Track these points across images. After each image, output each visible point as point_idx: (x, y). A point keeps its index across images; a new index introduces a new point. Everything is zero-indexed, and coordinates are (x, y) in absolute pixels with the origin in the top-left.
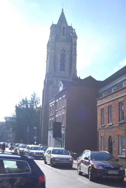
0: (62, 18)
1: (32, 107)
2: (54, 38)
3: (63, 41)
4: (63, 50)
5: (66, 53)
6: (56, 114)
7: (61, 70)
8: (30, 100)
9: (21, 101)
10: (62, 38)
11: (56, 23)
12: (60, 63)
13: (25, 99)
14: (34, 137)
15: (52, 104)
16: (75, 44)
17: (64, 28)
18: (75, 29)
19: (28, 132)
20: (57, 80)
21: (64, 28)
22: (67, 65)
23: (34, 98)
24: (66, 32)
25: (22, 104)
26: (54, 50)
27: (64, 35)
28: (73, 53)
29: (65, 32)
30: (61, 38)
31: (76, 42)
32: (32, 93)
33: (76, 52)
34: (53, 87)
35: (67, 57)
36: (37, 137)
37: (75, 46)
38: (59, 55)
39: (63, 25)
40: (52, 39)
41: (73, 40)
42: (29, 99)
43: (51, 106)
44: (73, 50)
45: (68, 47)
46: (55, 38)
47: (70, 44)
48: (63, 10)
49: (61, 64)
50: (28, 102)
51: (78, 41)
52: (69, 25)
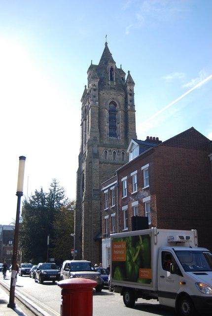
0: (107, 56)
1: (51, 203)
2: (96, 83)
3: (109, 93)
4: (112, 102)
7: (111, 134)
8: (49, 192)
9: (34, 194)
11: (97, 62)
13: (39, 191)
14: (72, 252)
15: (109, 188)
16: (132, 94)
17: (112, 69)
19: (48, 244)
20: (106, 151)
21: (112, 69)
22: (120, 126)
23: (55, 190)
24: (116, 76)
25: (35, 199)
27: (112, 79)
28: (129, 107)
29: (114, 76)
32: (52, 182)
33: (133, 106)
34: (100, 163)
35: (120, 113)
36: (76, 251)
38: (106, 110)
41: (128, 88)
42: (47, 191)
44: (129, 102)
45: (120, 99)
48: (106, 43)
51: (136, 89)
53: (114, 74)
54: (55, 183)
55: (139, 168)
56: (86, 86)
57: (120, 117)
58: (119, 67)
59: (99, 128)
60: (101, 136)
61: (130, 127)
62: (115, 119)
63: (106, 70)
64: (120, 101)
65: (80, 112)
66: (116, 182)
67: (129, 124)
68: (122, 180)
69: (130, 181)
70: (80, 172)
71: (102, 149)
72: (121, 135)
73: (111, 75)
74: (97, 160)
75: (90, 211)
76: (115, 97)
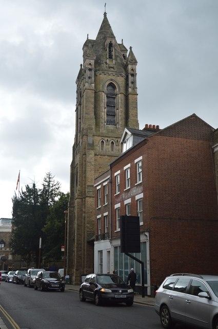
0: (105, 27)
1: (45, 202)
4: (111, 85)
6: (113, 204)
8: (42, 188)
9: (25, 190)
11: (93, 37)
13: (31, 187)
16: (134, 75)
17: (111, 45)
20: (103, 142)
21: (111, 45)
22: (120, 112)
23: (49, 185)
24: (115, 53)
27: (111, 57)
28: (130, 90)
29: (113, 53)
30: (106, 63)
32: (45, 176)
33: (135, 88)
35: (120, 98)
38: (103, 94)
40: (90, 64)
41: (130, 67)
42: (40, 187)
43: (99, 187)
44: (130, 84)
45: (120, 81)
48: (105, 14)
50: (37, 192)
53: (114, 50)
54: (50, 178)
55: (132, 161)
56: (81, 65)
57: (120, 101)
58: (119, 42)
59: (95, 114)
60: (97, 124)
61: (131, 112)
63: (104, 46)
64: (120, 83)
65: (75, 95)
66: (109, 177)
67: (130, 110)
68: (116, 174)
69: (123, 174)
70: (73, 166)
71: (98, 139)
72: (120, 123)
73: (110, 52)
74: (92, 152)
75: (83, 210)
76: (113, 78)
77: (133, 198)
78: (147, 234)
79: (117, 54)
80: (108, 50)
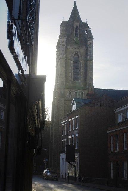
0: (75, 13)
2: (65, 40)
4: (76, 54)
5: (80, 58)
6: (68, 136)
10: (75, 40)
11: (67, 19)
12: (72, 72)
14: (44, 161)
16: (91, 47)
17: (77, 27)
18: (90, 28)
20: (70, 92)
21: (77, 27)
22: (81, 72)
26: (65, 55)
27: (76, 35)
28: (88, 58)
30: (74, 40)
31: (91, 44)
33: (91, 56)
34: (65, 100)
35: (81, 64)
36: (47, 160)
37: (90, 49)
39: (76, 24)
40: (63, 42)
41: (89, 42)
43: (63, 125)
44: (89, 54)
45: (82, 51)
46: (66, 41)
47: (84, 47)
48: (75, 2)
49: (74, 72)
52: (83, 21)
57: (82, 65)
62: (78, 67)
63: (73, 27)
66: (67, 121)
67: (88, 71)
73: (76, 31)
77: (75, 135)
78: (78, 153)
79: (81, 33)
80: (75, 31)
